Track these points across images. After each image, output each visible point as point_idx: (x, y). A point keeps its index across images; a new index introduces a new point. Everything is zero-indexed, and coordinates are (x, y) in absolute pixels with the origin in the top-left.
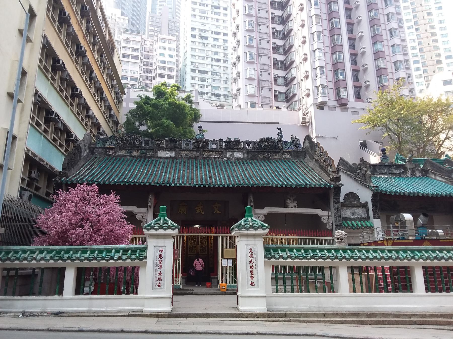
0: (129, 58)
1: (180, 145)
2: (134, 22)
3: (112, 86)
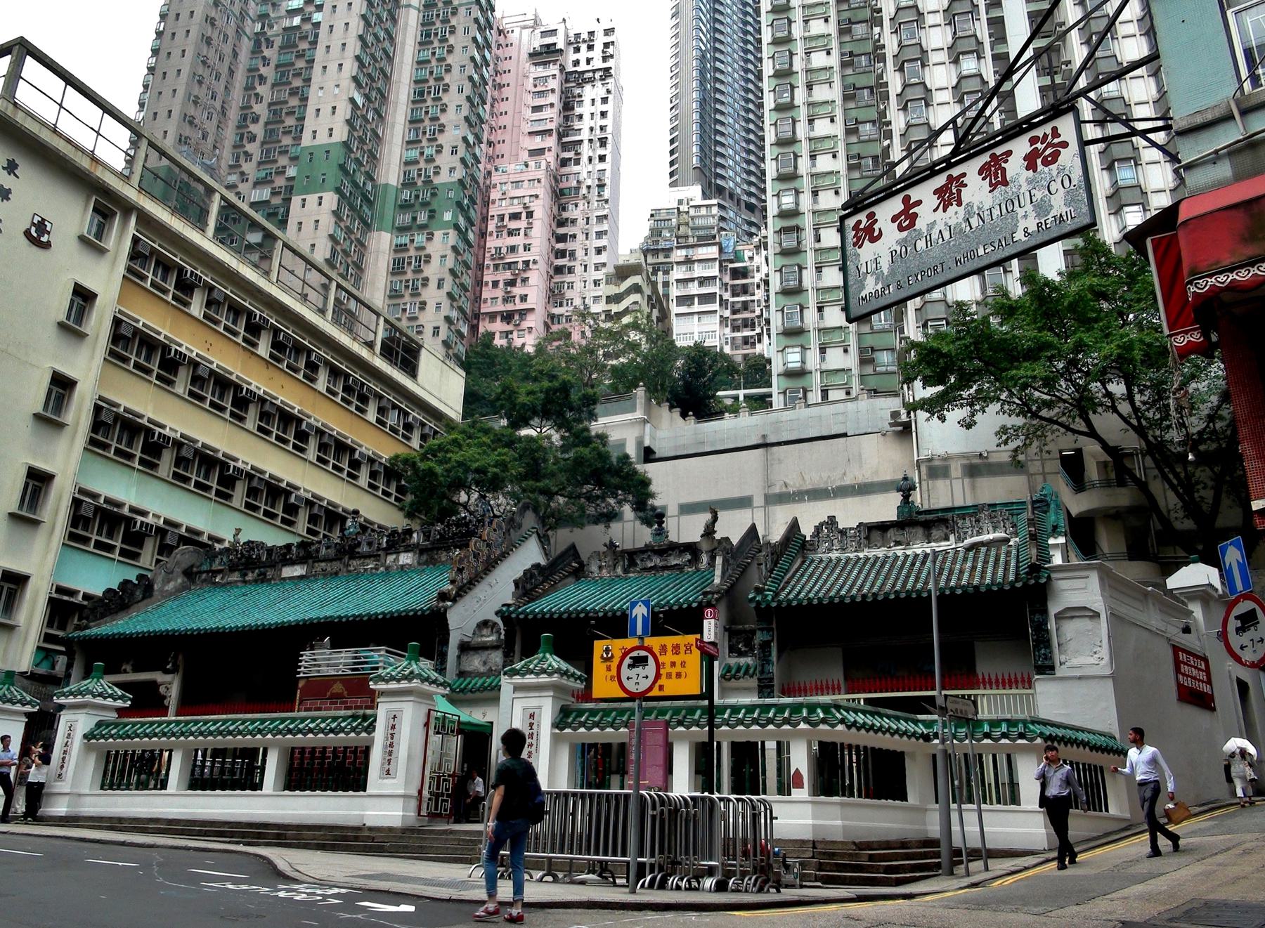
0: (693, 304)
1: (317, 551)
2: (753, 200)
3: (408, 427)
